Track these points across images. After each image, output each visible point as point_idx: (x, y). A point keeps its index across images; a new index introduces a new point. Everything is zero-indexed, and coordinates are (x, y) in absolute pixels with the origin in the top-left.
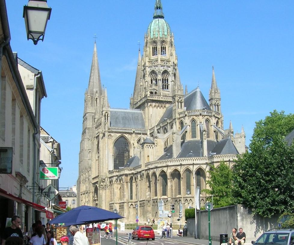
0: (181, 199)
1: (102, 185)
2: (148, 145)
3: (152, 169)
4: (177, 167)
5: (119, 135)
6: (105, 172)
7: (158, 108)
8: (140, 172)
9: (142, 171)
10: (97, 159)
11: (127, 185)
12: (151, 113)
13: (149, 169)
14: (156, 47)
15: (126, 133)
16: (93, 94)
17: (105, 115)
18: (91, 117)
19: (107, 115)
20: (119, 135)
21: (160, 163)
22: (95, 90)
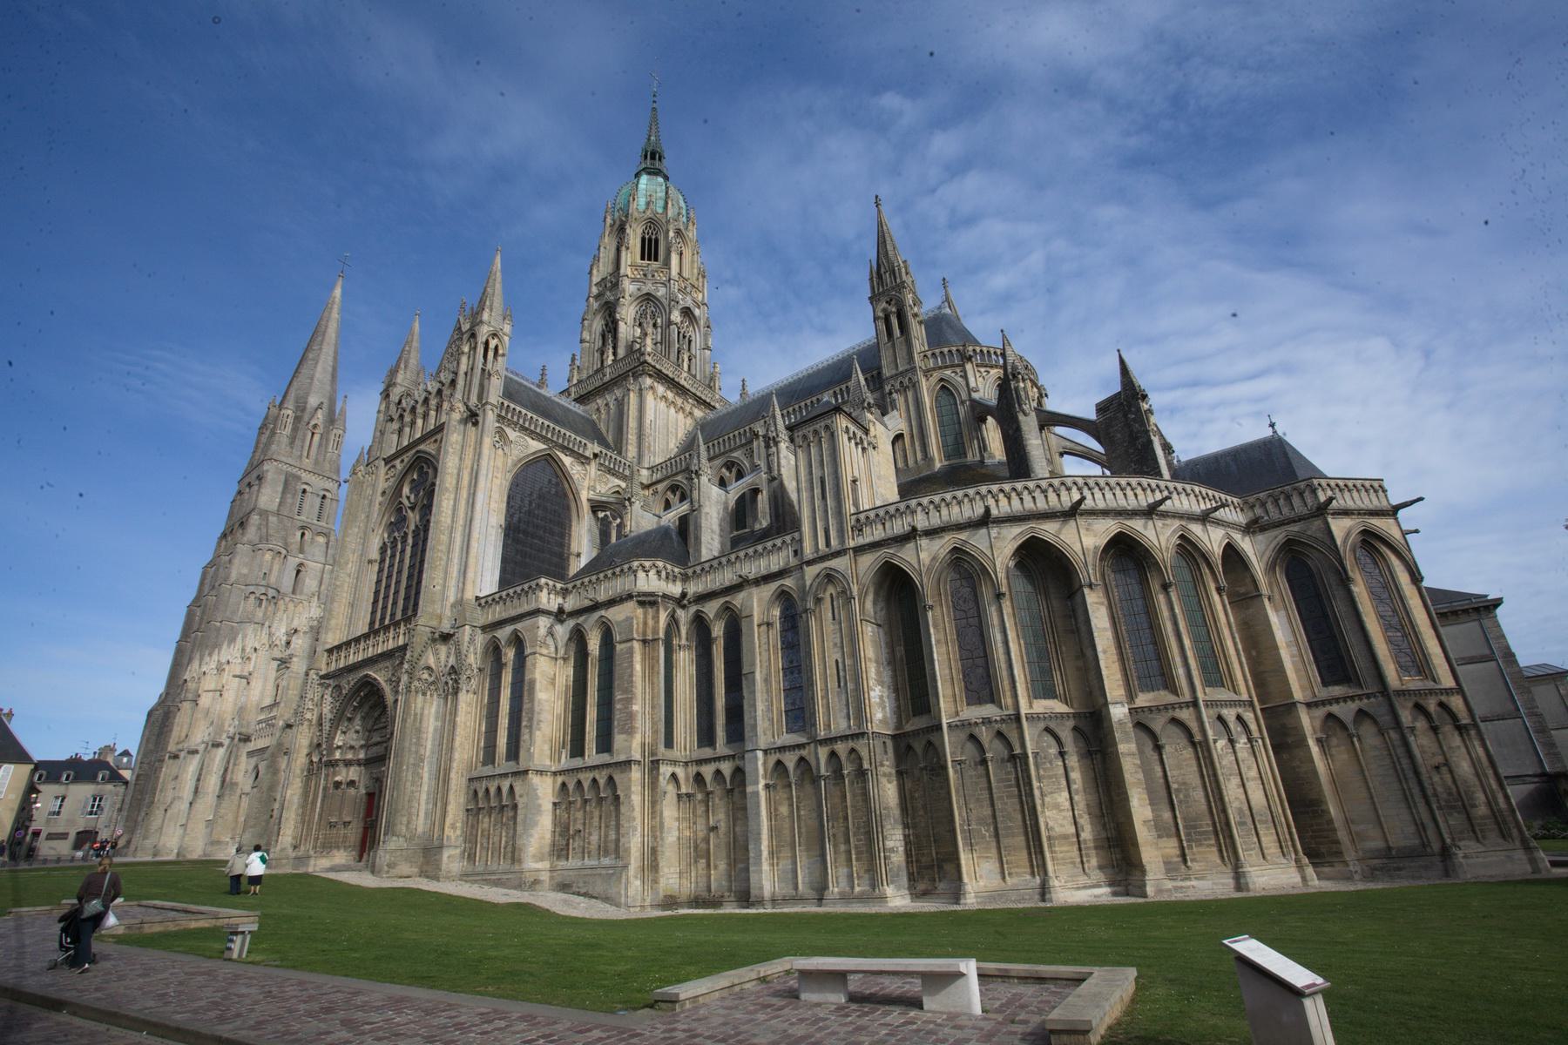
0: (1185, 715)
1: (429, 668)
2: (852, 428)
3: (931, 533)
4: (1129, 523)
5: (536, 446)
6: (452, 599)
7: (672, 410)
8: (781, 574)
9: (809, 563)
10: (375, 554)
11: (649, 661)
12: (649, 415)
13: (912, 535)
14: (657, 241)
15: (564, 449)
16: (304, 410)
17: (487, 344)
18: (283, 478)
19: (496, 348)
20: (536, 446)
21: (1009, 499)
22: (313, 401)
